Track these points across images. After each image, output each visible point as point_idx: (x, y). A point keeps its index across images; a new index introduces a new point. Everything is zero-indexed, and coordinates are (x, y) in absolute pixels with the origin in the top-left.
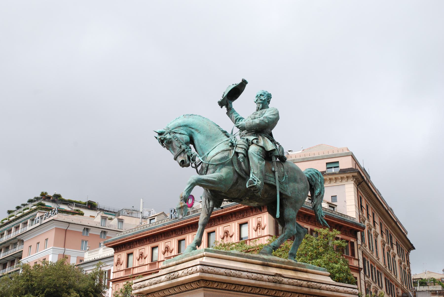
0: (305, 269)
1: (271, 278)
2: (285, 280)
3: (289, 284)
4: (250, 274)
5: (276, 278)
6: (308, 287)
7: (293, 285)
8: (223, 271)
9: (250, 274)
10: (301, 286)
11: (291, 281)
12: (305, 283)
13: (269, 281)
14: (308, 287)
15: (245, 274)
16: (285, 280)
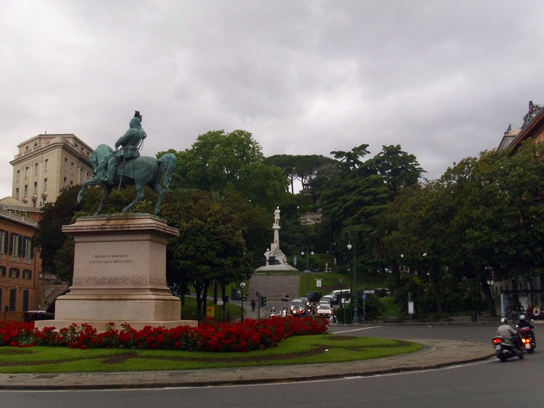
1: (99, 227)
2: (107, 227)
3: (110, 228)
4: (87, 227)
5: (103, 226)
6: (122, 228)
7: (112, 228)
8: (73, 228)
9: (87, 227)
10: (117, 228)
11: (110, 227)
12: (119, 226)
13: (98, 229)
15: (85, 227)
16: (107, 227)
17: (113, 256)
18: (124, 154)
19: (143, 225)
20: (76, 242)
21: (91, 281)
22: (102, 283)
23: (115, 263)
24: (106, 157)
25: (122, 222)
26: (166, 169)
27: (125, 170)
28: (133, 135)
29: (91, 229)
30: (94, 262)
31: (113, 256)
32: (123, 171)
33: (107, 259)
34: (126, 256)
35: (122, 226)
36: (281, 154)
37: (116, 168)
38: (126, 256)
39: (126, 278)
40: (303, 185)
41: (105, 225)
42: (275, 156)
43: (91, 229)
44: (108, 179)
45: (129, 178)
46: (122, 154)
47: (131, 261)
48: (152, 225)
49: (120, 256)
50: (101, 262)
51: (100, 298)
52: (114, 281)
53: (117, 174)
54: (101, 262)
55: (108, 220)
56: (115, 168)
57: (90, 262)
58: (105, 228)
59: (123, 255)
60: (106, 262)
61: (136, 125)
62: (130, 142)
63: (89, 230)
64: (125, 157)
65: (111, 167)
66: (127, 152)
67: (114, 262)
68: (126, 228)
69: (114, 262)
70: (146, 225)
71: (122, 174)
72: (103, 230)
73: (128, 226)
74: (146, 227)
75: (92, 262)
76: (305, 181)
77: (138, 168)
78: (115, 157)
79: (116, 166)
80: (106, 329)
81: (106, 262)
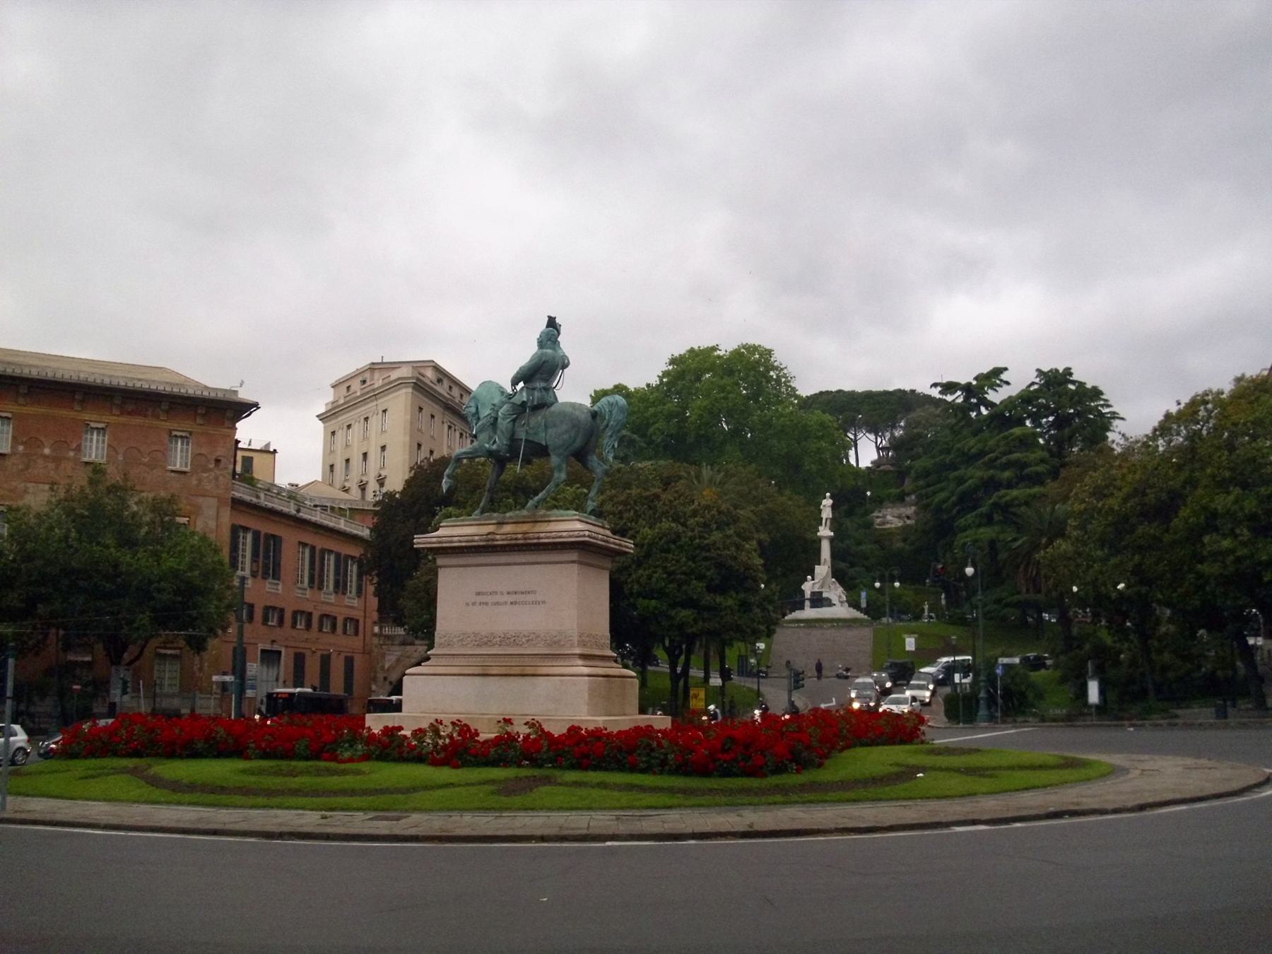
0: (547, 519)
2: (498, 537)
3: (503, 540)
4: (461, 538)
5: (489, 537)
6: (525, 539)
8: (434, 540)
9: (461, 538)
10: (516, 539)
11: (504, 537)
12: (519, 536)
13: (481, 540)
14: (525, 539)
15: (456, 539)
16: (498, 537)
17: (508, 593)
18: (528, 399)
19: (565, 534)
20: (441, 567)
21: (469, 639)
22: (489, 643)
23: (514, 606)
24: (494, 405)
25: (525, 528)
26: (607, 426)
27: (530, 428)
28: (544, 362)
29: (467, 542)
30: (474, 604)
31: (508, 593)
32: (527, 431)
33: (498, 598)
34: (534, 592)
35: (527, 535)
36: (834, 388)
37: (514, 425)
38: (534, 592)
39: (534, 633)
40: (878, 449)
41: (493, 533)
42: (821, 393)
43: (467, 542)
44: (498, 446)
45: (538, 444)
46: (525, 399)
47: (544, 602)
48: (581, 533)
49: (522, 593)
50: (486, 604)
51: (486, 672)
52: (512, 640)
53: (516, 437)
54: (486, 604)
55: (500, 524)
56: (510, 426)
57: (467, 604)
58: (493, 540)
59: (528, 590)
60: (497, 603)
61: (549, 343)
62: (538, 376)
63: (464, 544)
64: (529, 404)
65: (504, 424)
66: (533, 395)
67: (512, 603)
68: (534, 539)
69: (512, 603)
70: (571, 533)
71: (524, 438)
72: (490, 543)
73: (537, 535)
74: (570, 537)
75: (470, 604)
76: (881, 442)
77: (555, 426)
78: (510, 405)
79: (514, 421)
80: (497, 730)
81: (497, 603)
